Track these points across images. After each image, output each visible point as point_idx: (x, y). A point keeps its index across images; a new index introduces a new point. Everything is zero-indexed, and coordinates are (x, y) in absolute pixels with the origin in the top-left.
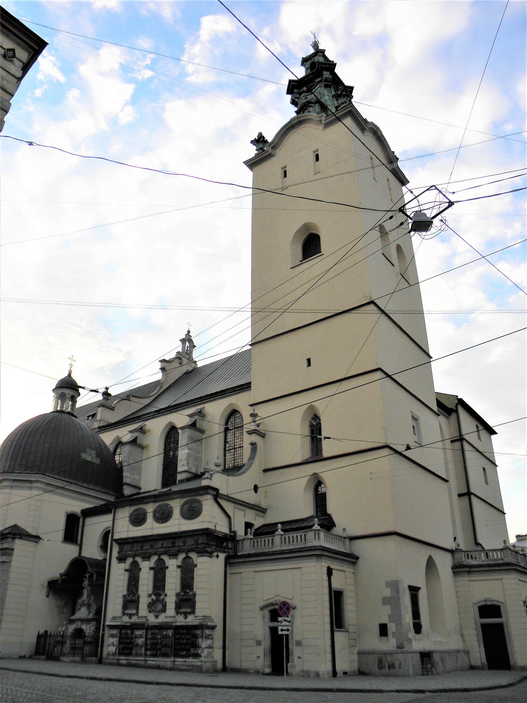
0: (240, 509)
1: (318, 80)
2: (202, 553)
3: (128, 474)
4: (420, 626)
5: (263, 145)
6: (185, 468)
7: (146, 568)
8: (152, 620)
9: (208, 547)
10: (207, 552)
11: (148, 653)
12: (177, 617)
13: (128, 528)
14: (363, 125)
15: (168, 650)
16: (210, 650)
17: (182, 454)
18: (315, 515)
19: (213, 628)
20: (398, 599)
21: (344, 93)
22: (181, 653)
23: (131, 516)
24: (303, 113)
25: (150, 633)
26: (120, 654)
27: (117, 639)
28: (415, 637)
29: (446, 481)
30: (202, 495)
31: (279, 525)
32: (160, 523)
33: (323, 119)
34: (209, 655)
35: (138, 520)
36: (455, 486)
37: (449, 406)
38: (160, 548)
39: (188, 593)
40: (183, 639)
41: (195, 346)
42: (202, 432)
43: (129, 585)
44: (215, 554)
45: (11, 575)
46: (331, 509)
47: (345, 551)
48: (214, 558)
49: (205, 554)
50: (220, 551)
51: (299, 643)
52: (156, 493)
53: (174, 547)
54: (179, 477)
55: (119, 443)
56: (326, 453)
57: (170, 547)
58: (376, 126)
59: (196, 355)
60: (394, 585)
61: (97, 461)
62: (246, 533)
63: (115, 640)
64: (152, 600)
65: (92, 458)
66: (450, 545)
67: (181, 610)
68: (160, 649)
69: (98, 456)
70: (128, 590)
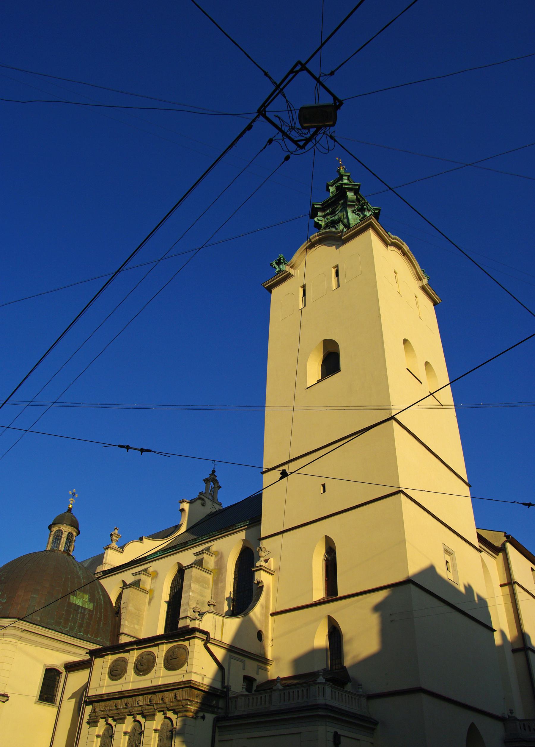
0: (238, 660)
9: (190, 705)
21: (365, 207)
32: (141, 675)
41: (220, 487)
48: (200, 721)
57: (148, 705)
65: (84, 602)
69: (91, 600)
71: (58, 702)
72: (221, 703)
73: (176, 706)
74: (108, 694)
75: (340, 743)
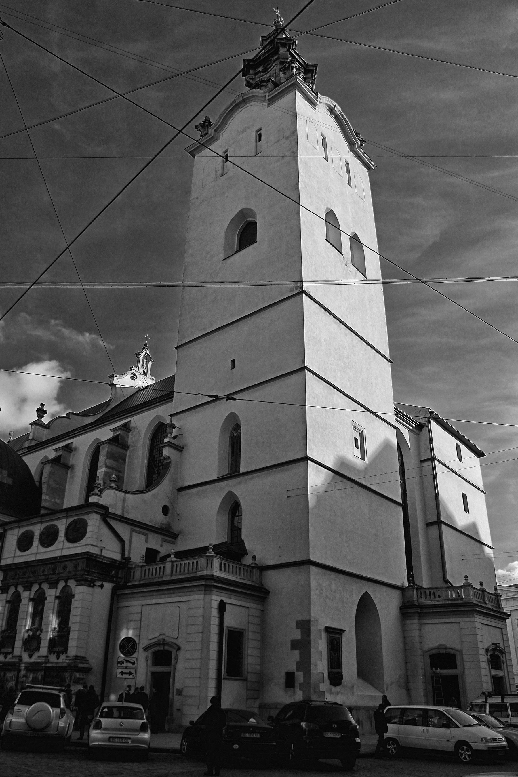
1: (275, 58)
2: (80, 582)
3: (47, 498)
4: (341, 677)
9: (86, 575)
10: (86, 580)
12: (49, 656)
13: (15, 553)
28: (331, 690)
44: (98, 583)
49: (83, 582)
50: (106, 581)
51: (180, 692)
67: (55, 649)
69: (9, 475)
72: (120, 574)
75: (225, 610)
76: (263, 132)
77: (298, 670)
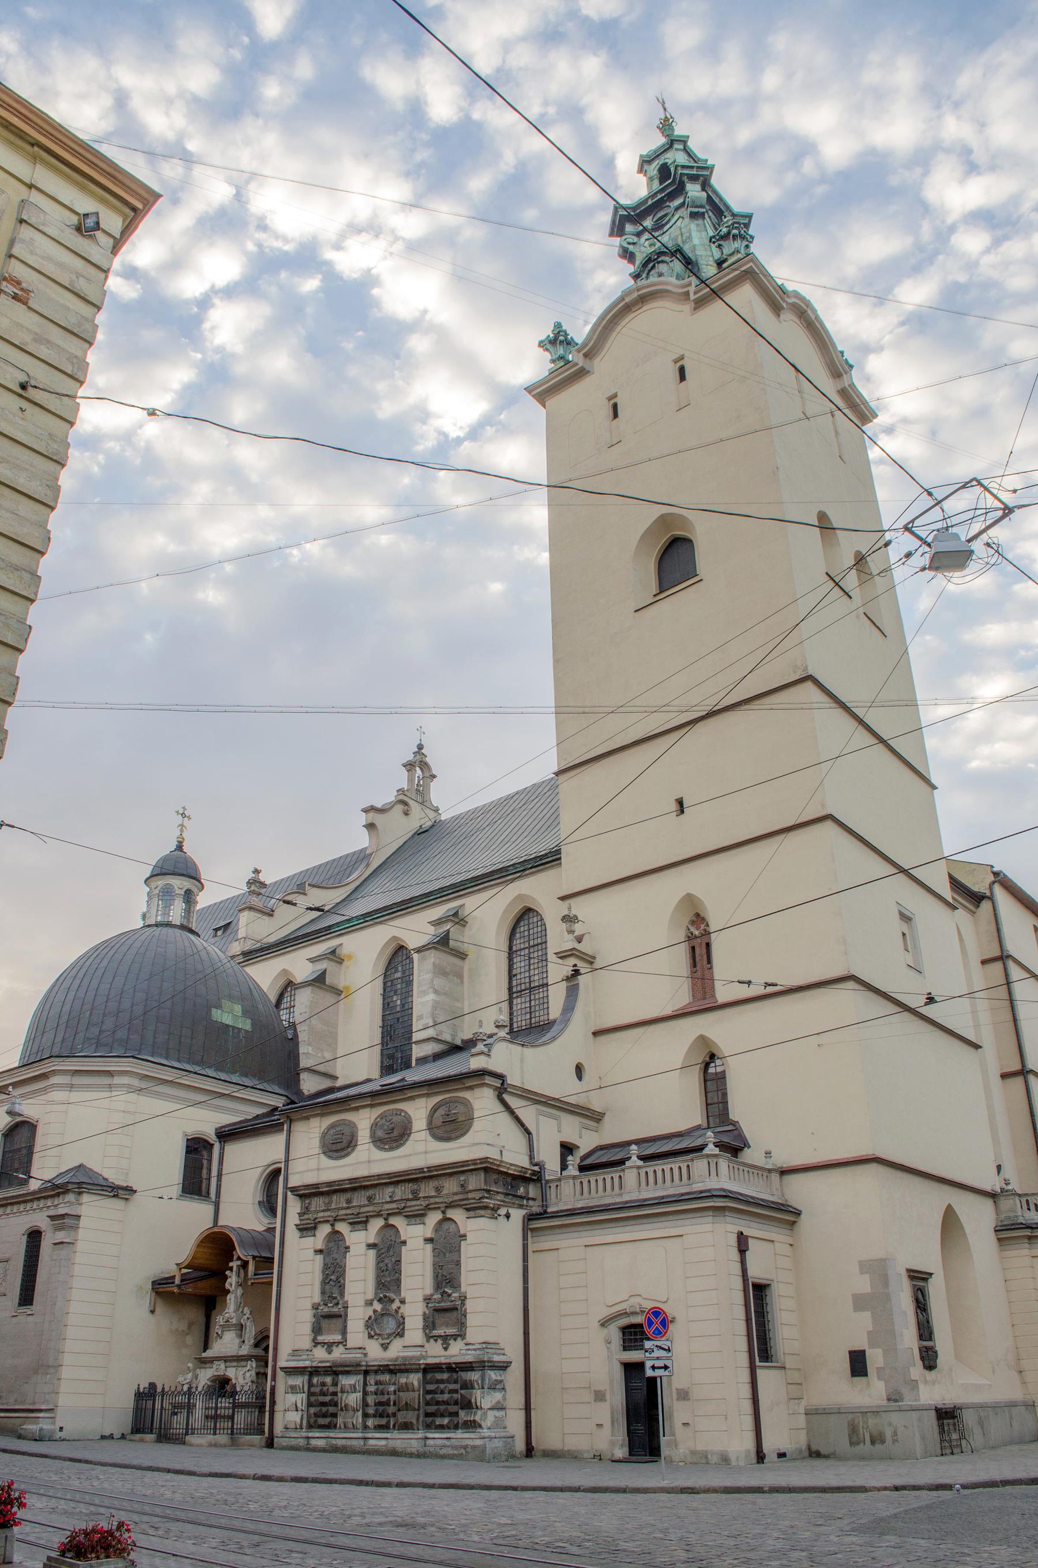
2: (473, 1209)
3: (310, 1050)
5: (565, 351)
6: (430, 1033)
7: (359, 1243)
8: (376, 1353)
11: (370, 1422)
12: (427, 1345)
14: (776, 298)
15: (410, 1416)
16: (498, 1413)
17: (424, 1003)
18: (705, 1125)
19: (504, 1367)
20: (887, 1298)
22: (439, 1421)
23: (324, 1136)
24: (647, 278)
25: (372, 1382)
26: (310, 1427)
27: (305, 1396)
29: (977, 1047)
30: (471, 1088)
31: (634, 1147)
32: (386, 1150)
33: (692, 289)
34: (499, 1424)
35: (339, 1145)
36: (995, 1056)
37: (975, 889)
38: (387, 1202)
39: (449, 1295)
40: (442, 1392)
41: (434, 776)
42: (462, 956)
43: (325, 1282)
44: (503, 1211)
45: (77, 1270)
46: (737, 1112)
47: (772, 1199)
48: (502, 1220)
49: (482, 1212)
50: (513, 1205)
51: (684, 1395)
52: (375, 1086)
53: (418, 1199)
54: (418, 1052)
55: (289, 986)
56: (723, 994)
58: (803, 299)
59: (437, 794)
60: (877, 1269)
61: (246, 1025)
62: (564, 1166)
63: (300, 1399)
64: (375, 1311)
66: (990, 1182)
67: (435, 1332)
68: (394, 1415)
69: (246, 1013)
70: (323, 1293)
71: (213, 1195)
72: (533, 1191)
73: (463, 1200)
74: (329, 1184)
76: (686, 363)
77: (872, 1345)
